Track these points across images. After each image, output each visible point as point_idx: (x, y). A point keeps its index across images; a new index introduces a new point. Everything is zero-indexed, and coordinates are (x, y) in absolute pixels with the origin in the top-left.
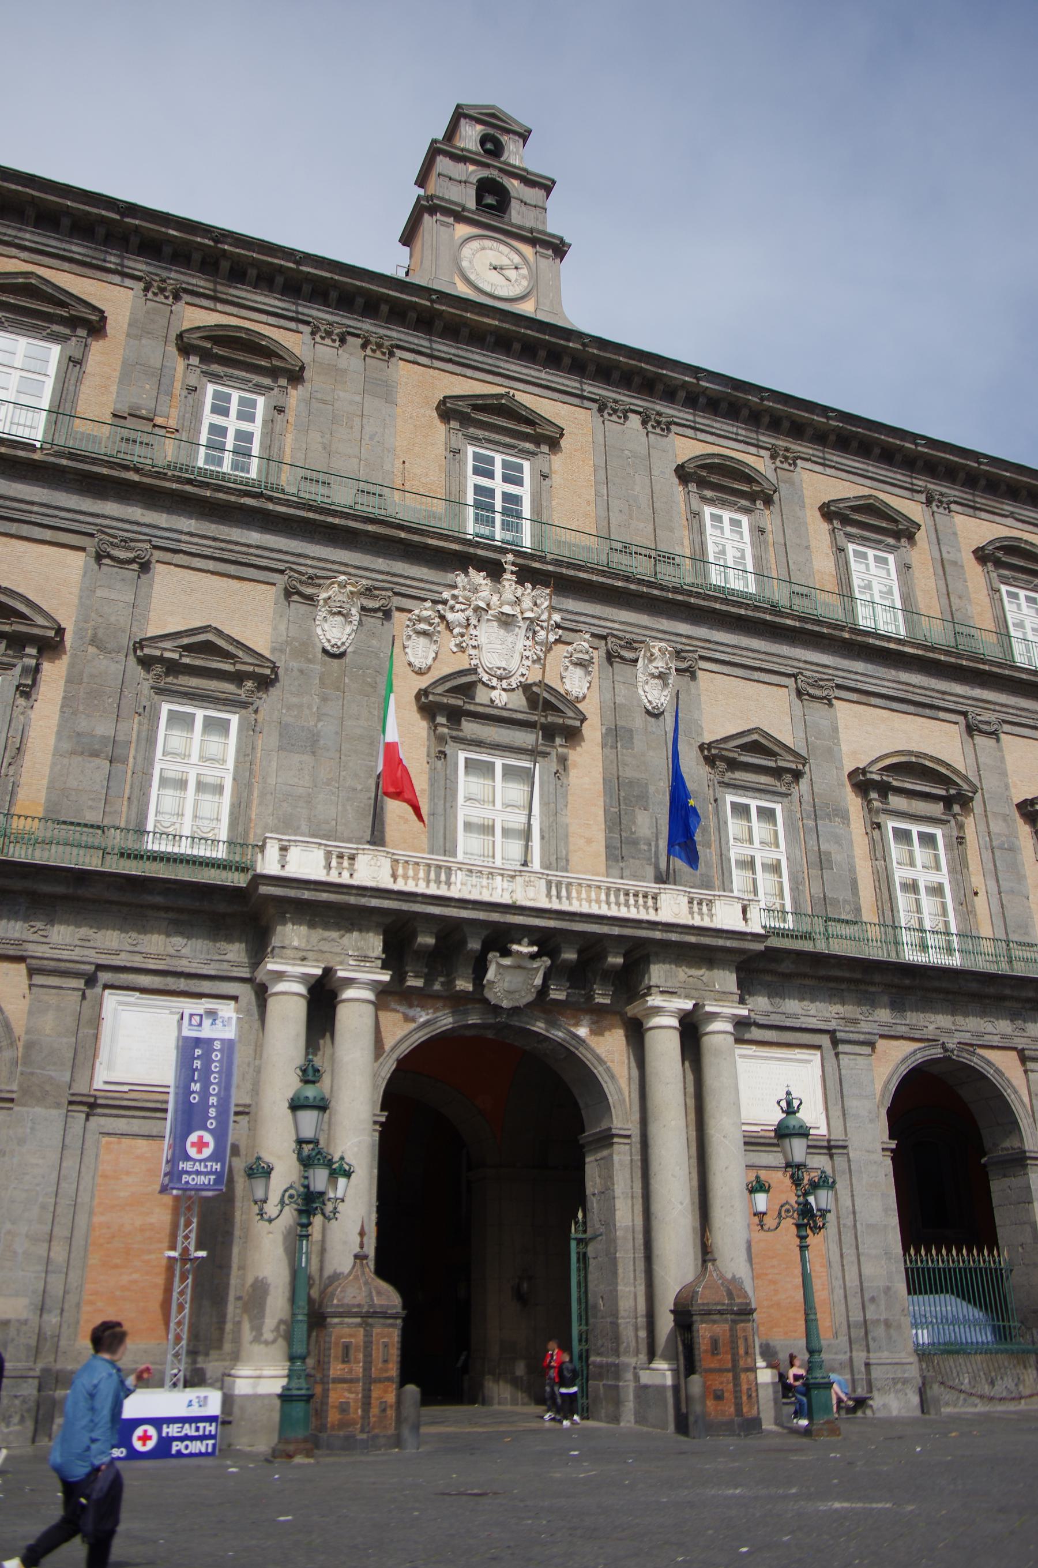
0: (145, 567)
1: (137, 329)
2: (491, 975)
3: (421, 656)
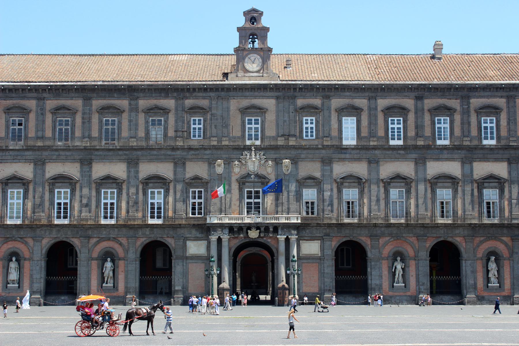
0: (184, 164)
1: (176, 109)
3: (237, 170)
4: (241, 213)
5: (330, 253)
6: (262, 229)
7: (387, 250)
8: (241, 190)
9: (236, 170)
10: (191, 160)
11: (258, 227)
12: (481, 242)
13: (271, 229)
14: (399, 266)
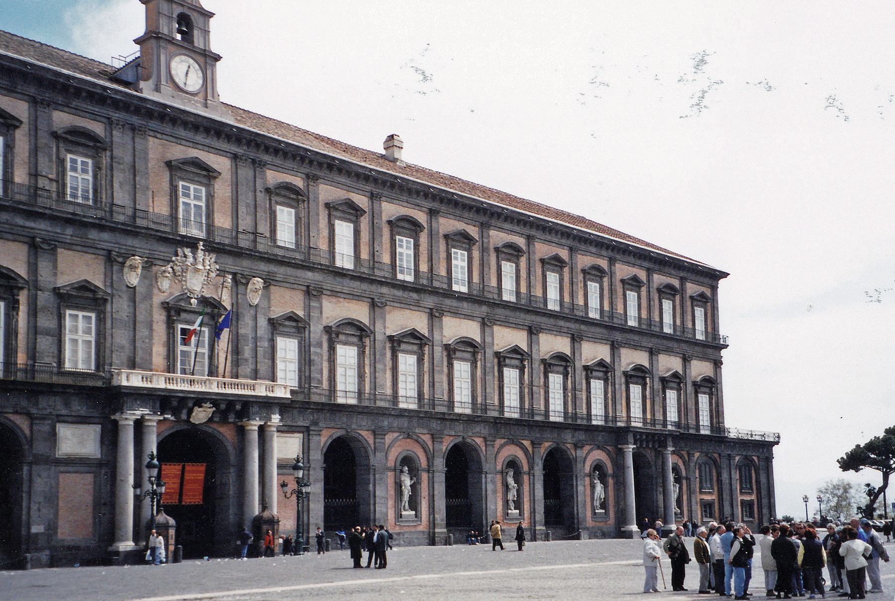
2: (194, 414)
4: (171, 368)
5: (317, 456)
6: (223, 406)
7: (394, 455)
8: (170, 324)
9: (165, 284)
10: (69, 246)
11: (215, 400)
12: (502, 446)
13: (238, 407)
14: (407, 482)
